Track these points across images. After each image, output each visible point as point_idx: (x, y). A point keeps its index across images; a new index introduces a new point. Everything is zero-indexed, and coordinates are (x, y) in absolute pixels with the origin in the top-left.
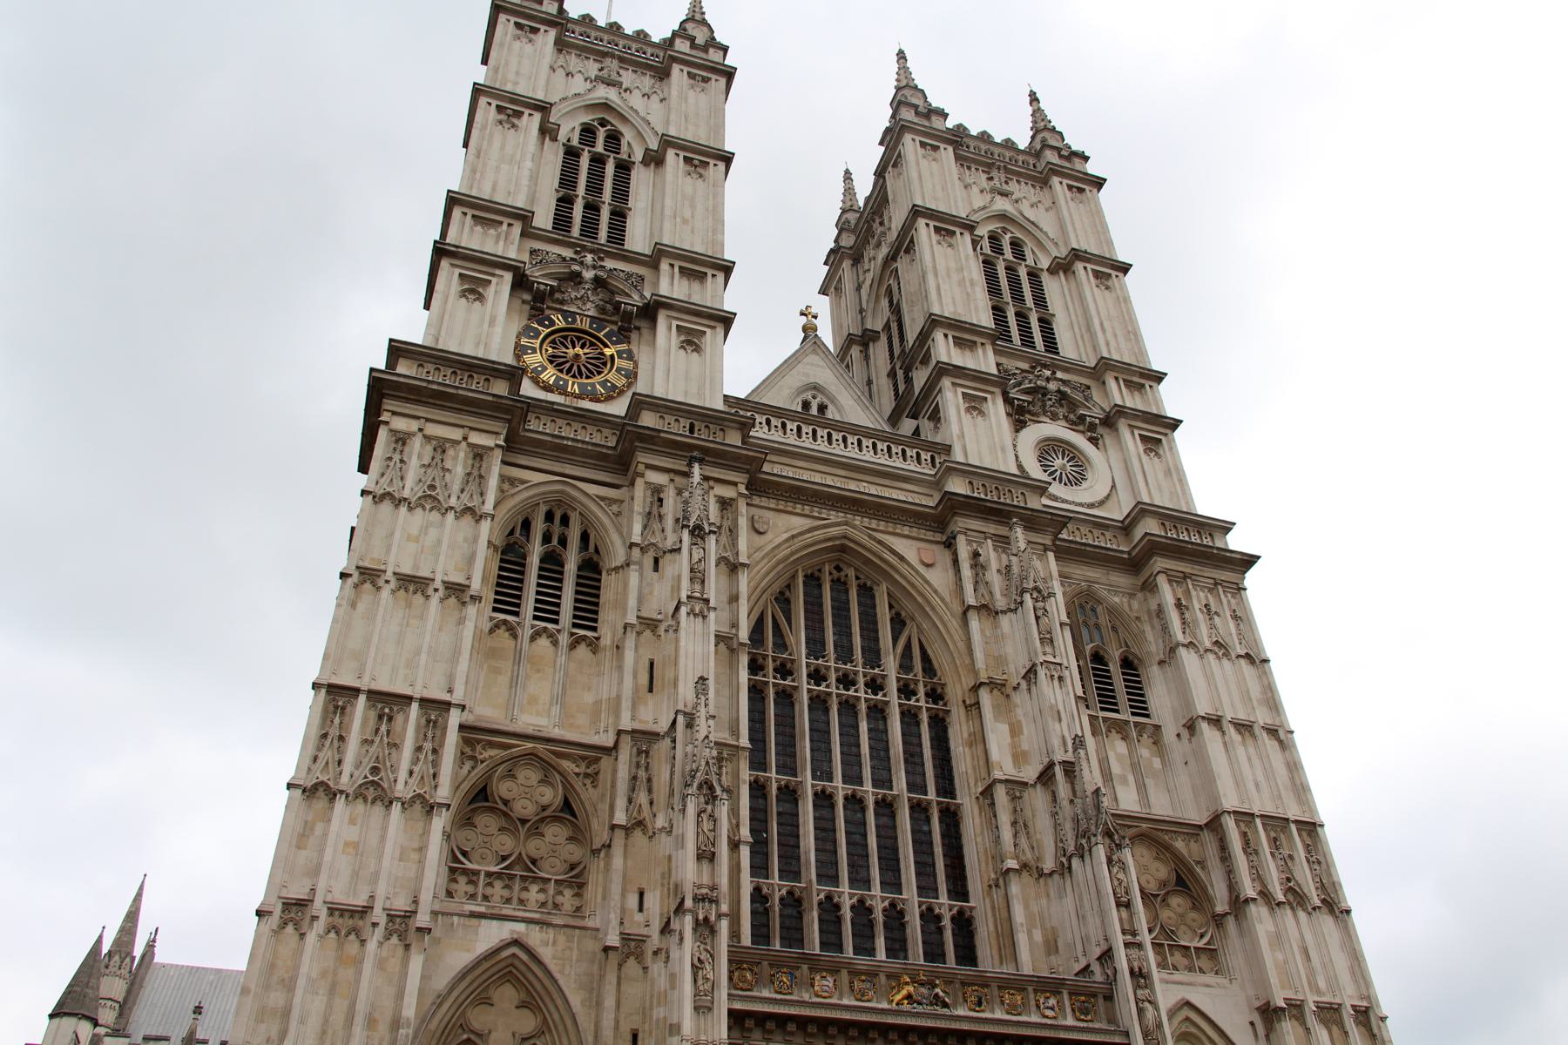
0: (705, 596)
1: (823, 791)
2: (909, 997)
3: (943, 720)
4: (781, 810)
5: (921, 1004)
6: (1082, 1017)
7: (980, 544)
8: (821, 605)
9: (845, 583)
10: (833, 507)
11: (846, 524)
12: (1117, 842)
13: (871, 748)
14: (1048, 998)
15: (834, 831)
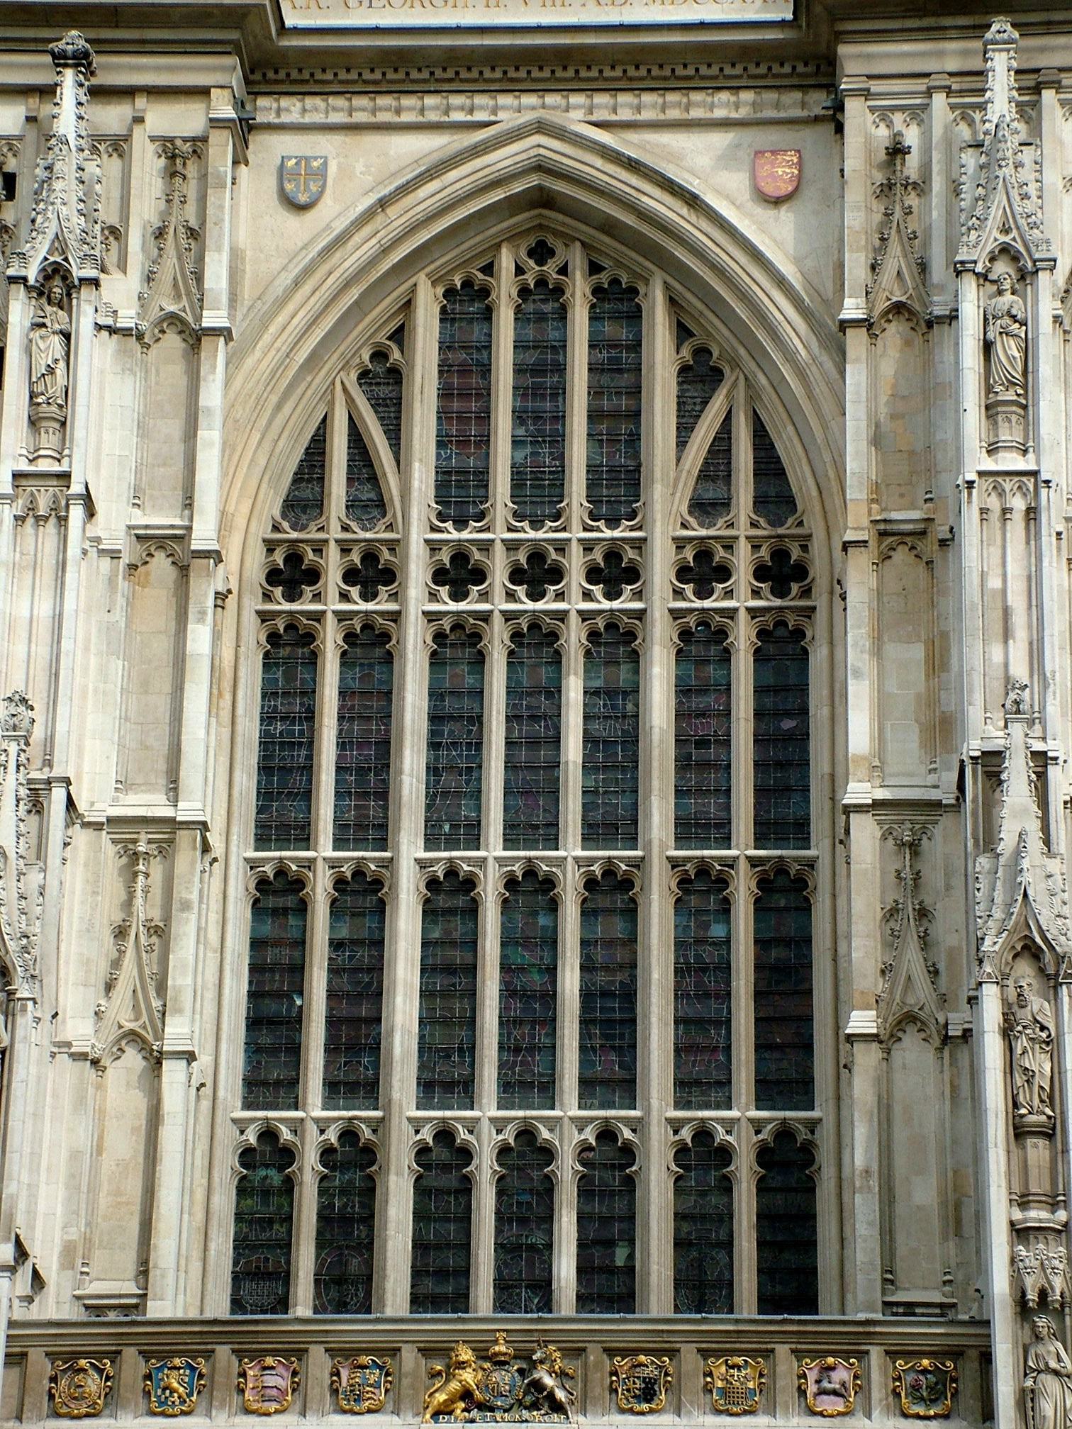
0: (64, 467)
1: (452, 872)
2: (466, 1395)
3: (799, 634)
4: (344, 933)
5: (492, 1409)
6: (920, 1410)
7: (919, 113)
8: (486, 370)
9: (559, 291)
10: (511, 86)
11: (541, 127)
12: (1051, 971)
13: (590, 740)
14: (832, 1368)
15: (471, 970)
